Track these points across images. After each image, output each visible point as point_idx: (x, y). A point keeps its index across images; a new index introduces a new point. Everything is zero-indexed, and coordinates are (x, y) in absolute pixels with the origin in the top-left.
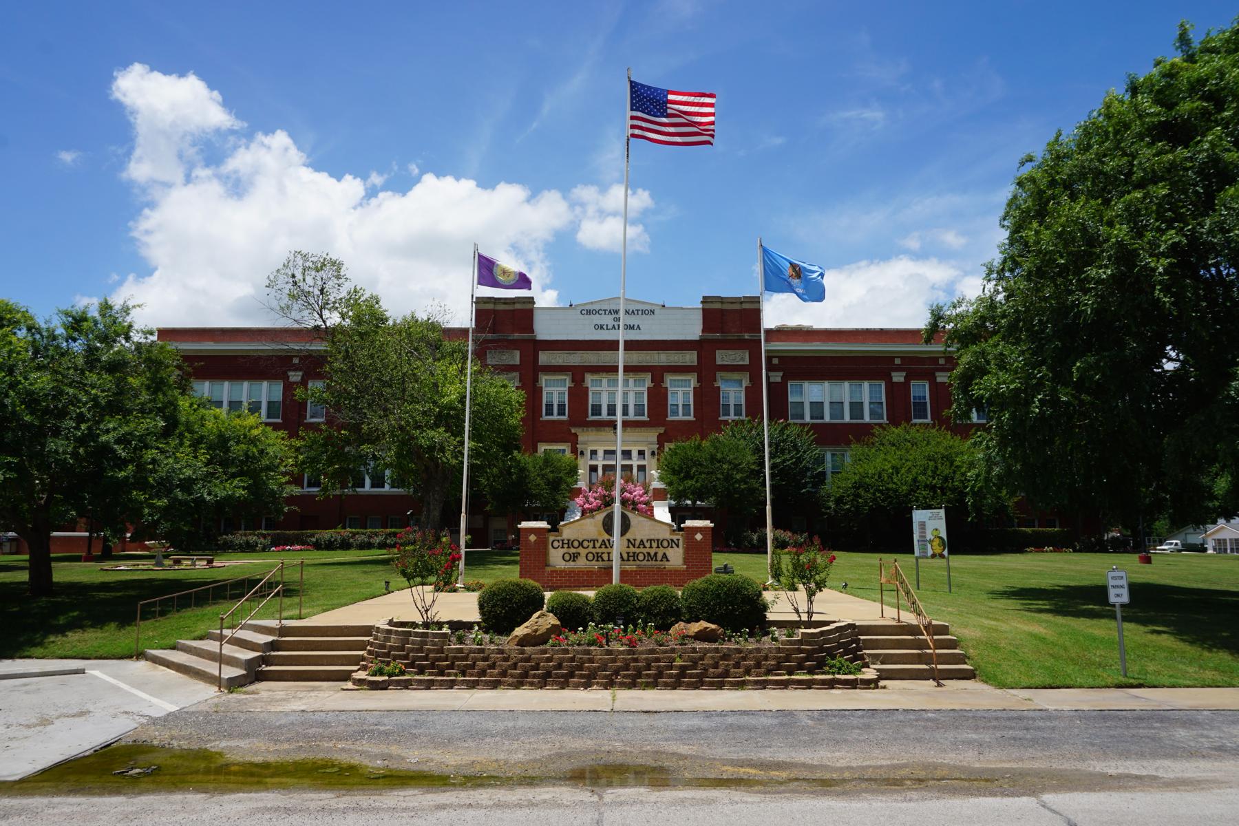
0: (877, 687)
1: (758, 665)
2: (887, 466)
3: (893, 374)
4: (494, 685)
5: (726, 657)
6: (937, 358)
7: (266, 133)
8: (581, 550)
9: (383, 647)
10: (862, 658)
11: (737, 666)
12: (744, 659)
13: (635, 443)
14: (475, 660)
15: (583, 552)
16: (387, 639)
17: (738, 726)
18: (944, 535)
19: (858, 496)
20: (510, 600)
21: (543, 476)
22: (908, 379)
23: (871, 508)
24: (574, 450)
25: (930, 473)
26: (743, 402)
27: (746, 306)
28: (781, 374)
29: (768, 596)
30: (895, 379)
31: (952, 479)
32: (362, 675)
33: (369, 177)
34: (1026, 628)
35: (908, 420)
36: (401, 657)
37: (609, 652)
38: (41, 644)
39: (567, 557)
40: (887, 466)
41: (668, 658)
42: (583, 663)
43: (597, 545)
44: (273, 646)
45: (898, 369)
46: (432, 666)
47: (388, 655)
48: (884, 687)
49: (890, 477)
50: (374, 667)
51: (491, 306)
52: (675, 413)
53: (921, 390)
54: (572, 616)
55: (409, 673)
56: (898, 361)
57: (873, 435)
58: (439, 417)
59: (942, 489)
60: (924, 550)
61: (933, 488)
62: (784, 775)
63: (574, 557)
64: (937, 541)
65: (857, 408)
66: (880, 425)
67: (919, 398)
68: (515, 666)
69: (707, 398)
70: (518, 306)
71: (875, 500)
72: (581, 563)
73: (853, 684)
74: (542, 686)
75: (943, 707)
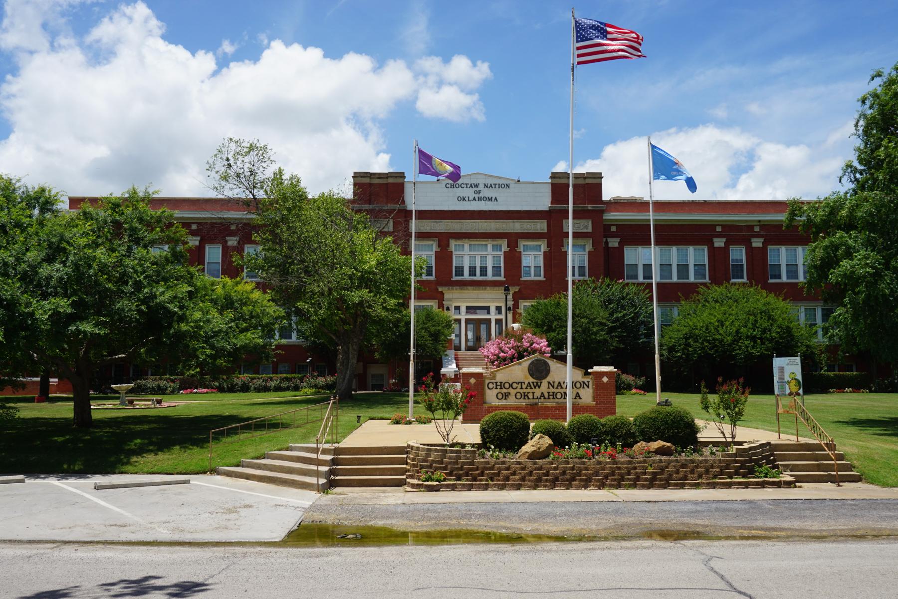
0: (795, 487)
1: (707, 472)
2: (714, 320)
3: (715, 240)
4: (518, 487)
5: (684, 466)
6: (753, 226)
7: (128, 4)
8: (511, 390)
9: (426, 461)
10: (776, 467)
11: (692, 472)
12: (697, 467)
13: (493, 300)
14: (500, 470)
15: (513, 392)
16: (428, 455)
17: (722, 507)
18: (800, 377)
19: (689, 345)
20: (511, 426)
21: (426, 329)
22: (727, 244)
23: (700, 356)
24: (441, 306)
25: (750, 325)
26: (586, 265)
27: (589, 181)
28: (618, 240)
29: (699, 423)
30: (716, 245)
31: (770, 330)
32: (415, 481)
33: (220, 45)
34: (887, 447)
35: (728, 280)
36: (441, 468)
37: (599, 463)
38: (128, 463)
39: (500, 396)
40: (714, 320)
41: (643, 467)
42: (581, 471)
43: (524, 386)
44: (334, 462)
45: (719, 236)
46: (467, 474)
47: (430, 467)
48: (800, 487)
49: (716, 329)
50: (423, 476)
51: (366, 180)
52: (529, 274)
53: (738, 254)
54: (559, 440)
55: (450, 480)
56: (719, 229)
57: (698, 293)
58: (361, 279)
59: (761, 339)
60: (782, 389)
61: (753, 338)
62: (784, 534)
63: (506, 396)
64: (794, 382)
65: (683, 269)
66: (704, 284)
67: (737, 260)
68: (531, 474)
69: (555, 261)
70: (391, 180)
71: (703, 348)
72: (511, 401)
73: (778, 485)
74: (553, 487)
75: (858, 498)
